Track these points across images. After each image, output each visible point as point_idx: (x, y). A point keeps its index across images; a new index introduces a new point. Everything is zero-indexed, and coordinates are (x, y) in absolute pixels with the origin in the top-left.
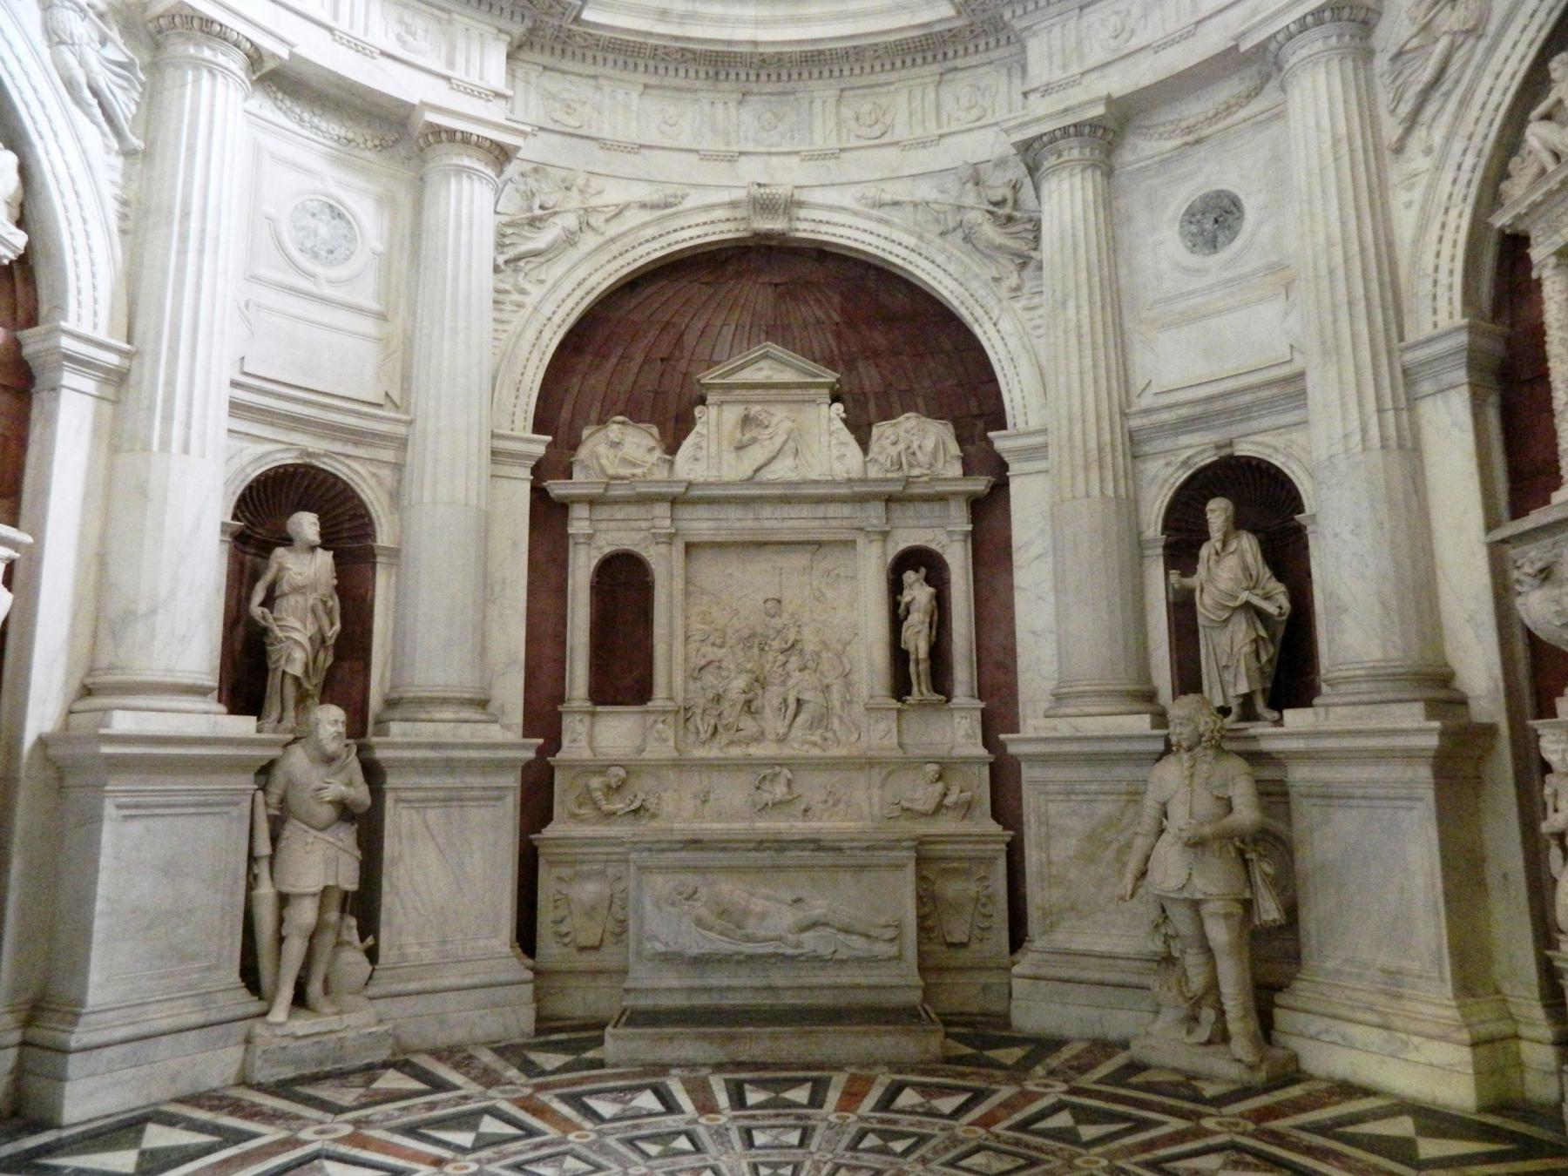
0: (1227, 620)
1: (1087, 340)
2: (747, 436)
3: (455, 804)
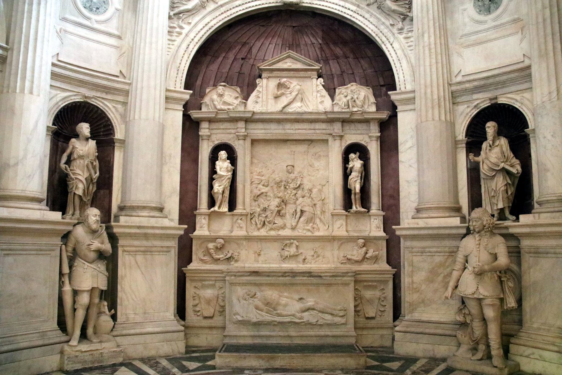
0: (494, 176)
1: (433, 50)
3: (149, 253)
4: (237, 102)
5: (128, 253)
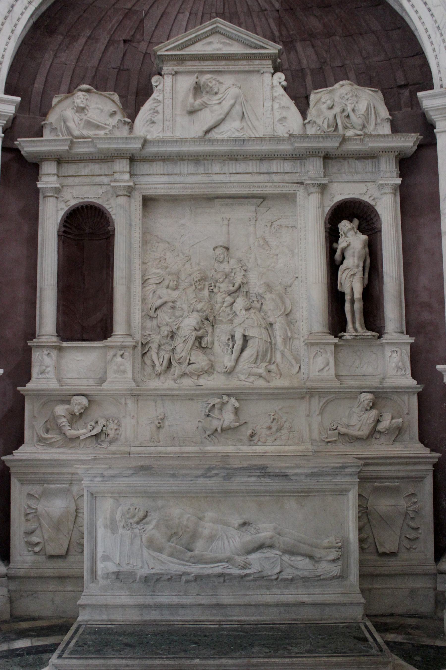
2: (198, 102)
4: (114, 121)
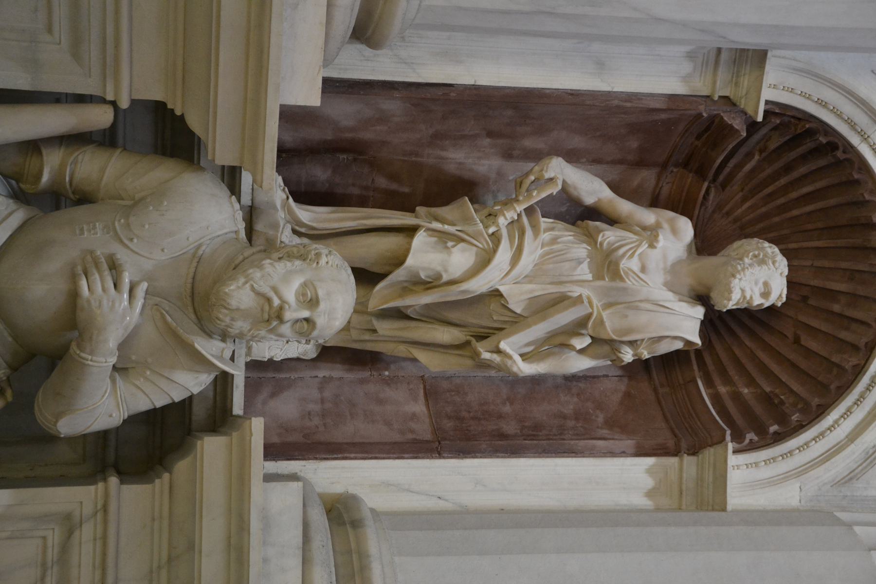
5: (52, 554)
